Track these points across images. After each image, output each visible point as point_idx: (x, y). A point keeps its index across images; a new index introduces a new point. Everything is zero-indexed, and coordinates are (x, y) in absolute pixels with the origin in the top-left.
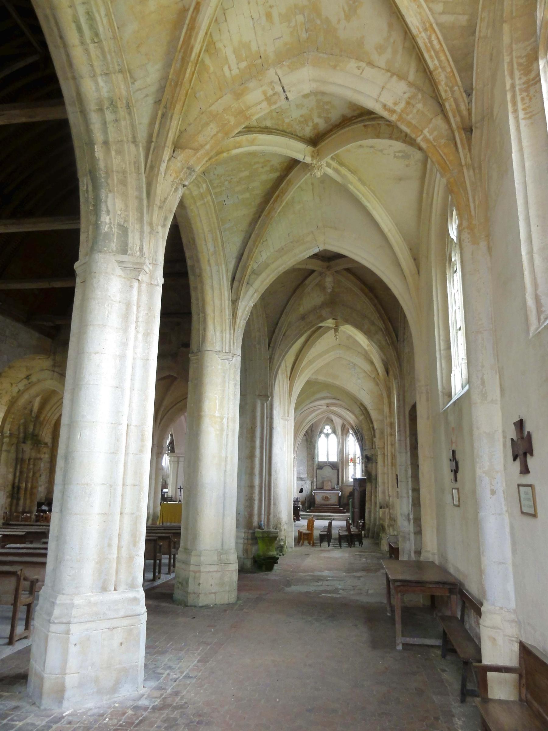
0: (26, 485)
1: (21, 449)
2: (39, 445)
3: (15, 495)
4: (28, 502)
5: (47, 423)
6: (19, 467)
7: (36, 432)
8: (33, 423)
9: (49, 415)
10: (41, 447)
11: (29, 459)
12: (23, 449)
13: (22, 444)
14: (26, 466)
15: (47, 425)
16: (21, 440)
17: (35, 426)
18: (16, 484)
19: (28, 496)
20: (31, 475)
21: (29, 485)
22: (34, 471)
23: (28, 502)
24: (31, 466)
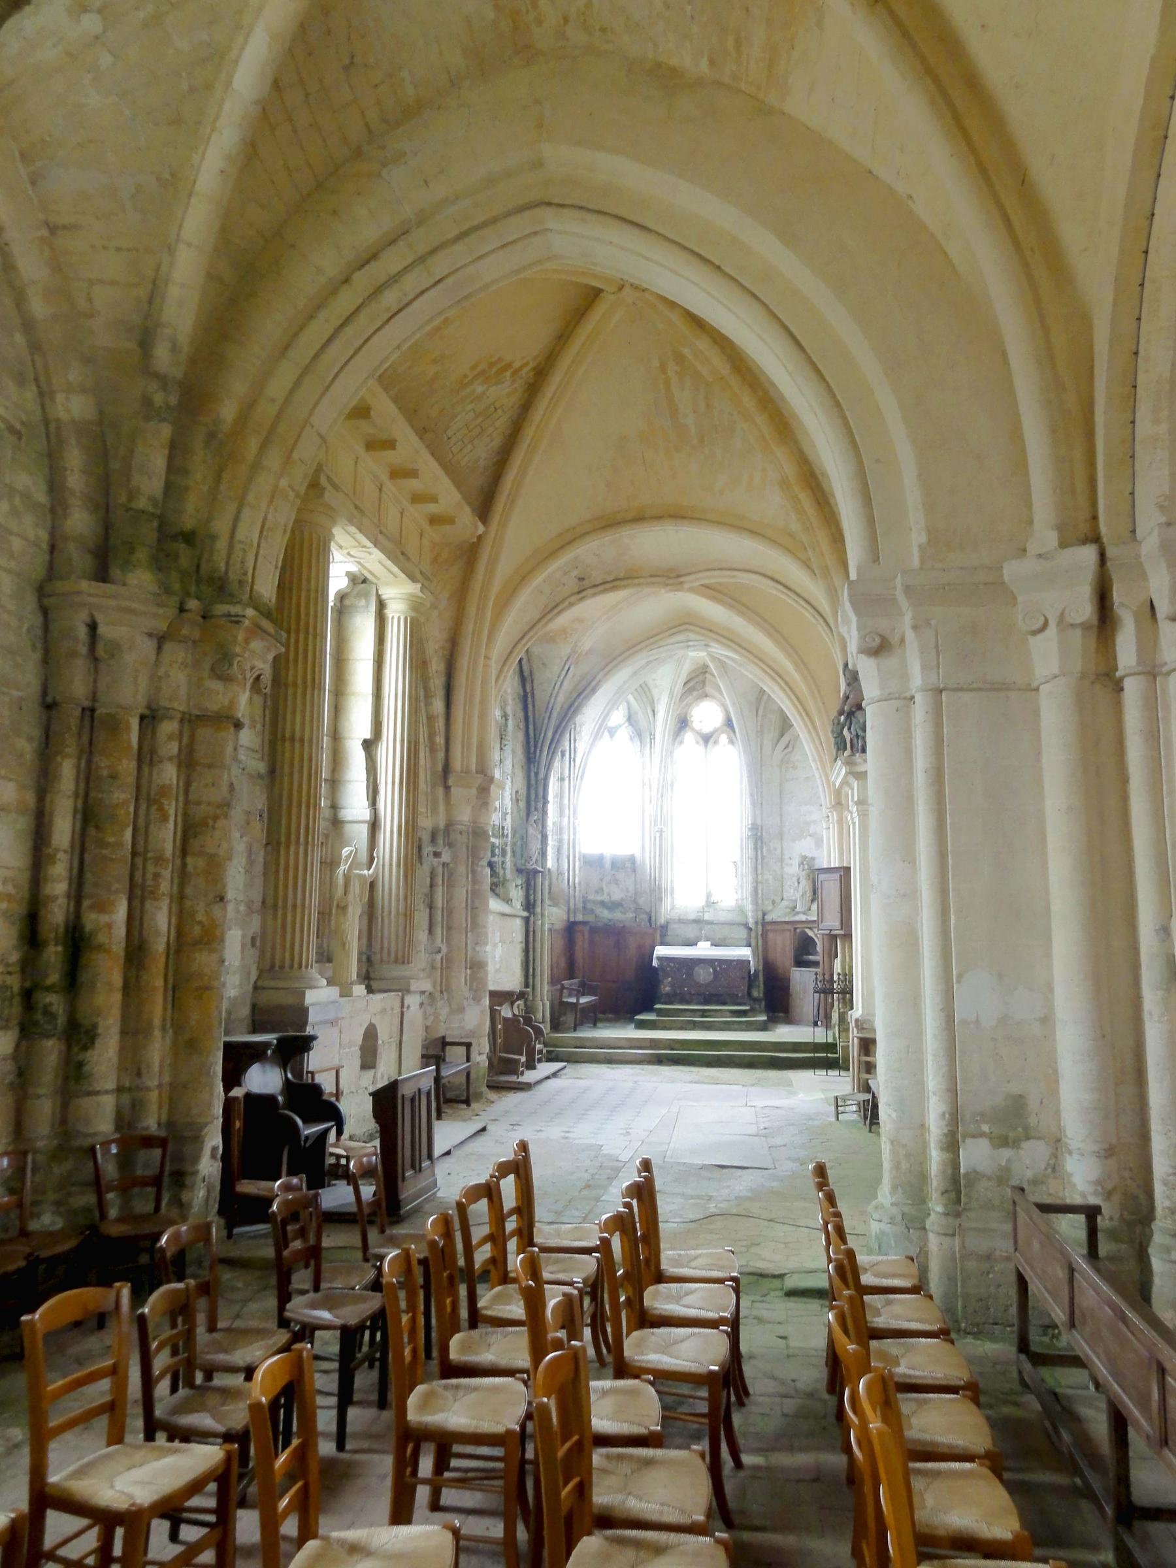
0: (134, 920)
1: (82, 632)
2: (220, 609)
3: (55, 1001)
4: (157, 1051)
5: (264, 445)
6: (67, 772)
7: (189, 515)
8: (166, 431)
9: (277, 388)
10: (236, 620)
11: (150, 719)
12: (93, 627)
13: (84, 585)
14: (127, 766)
15: (273, 460)
16: (79, 558)
17: (177, 451)
18: (56, 914)
19: (157, 1008)
20: (166, 837)
21: (161, 919)
22: (186, 815)
23: (157, 1051)
24: (169, 774)
